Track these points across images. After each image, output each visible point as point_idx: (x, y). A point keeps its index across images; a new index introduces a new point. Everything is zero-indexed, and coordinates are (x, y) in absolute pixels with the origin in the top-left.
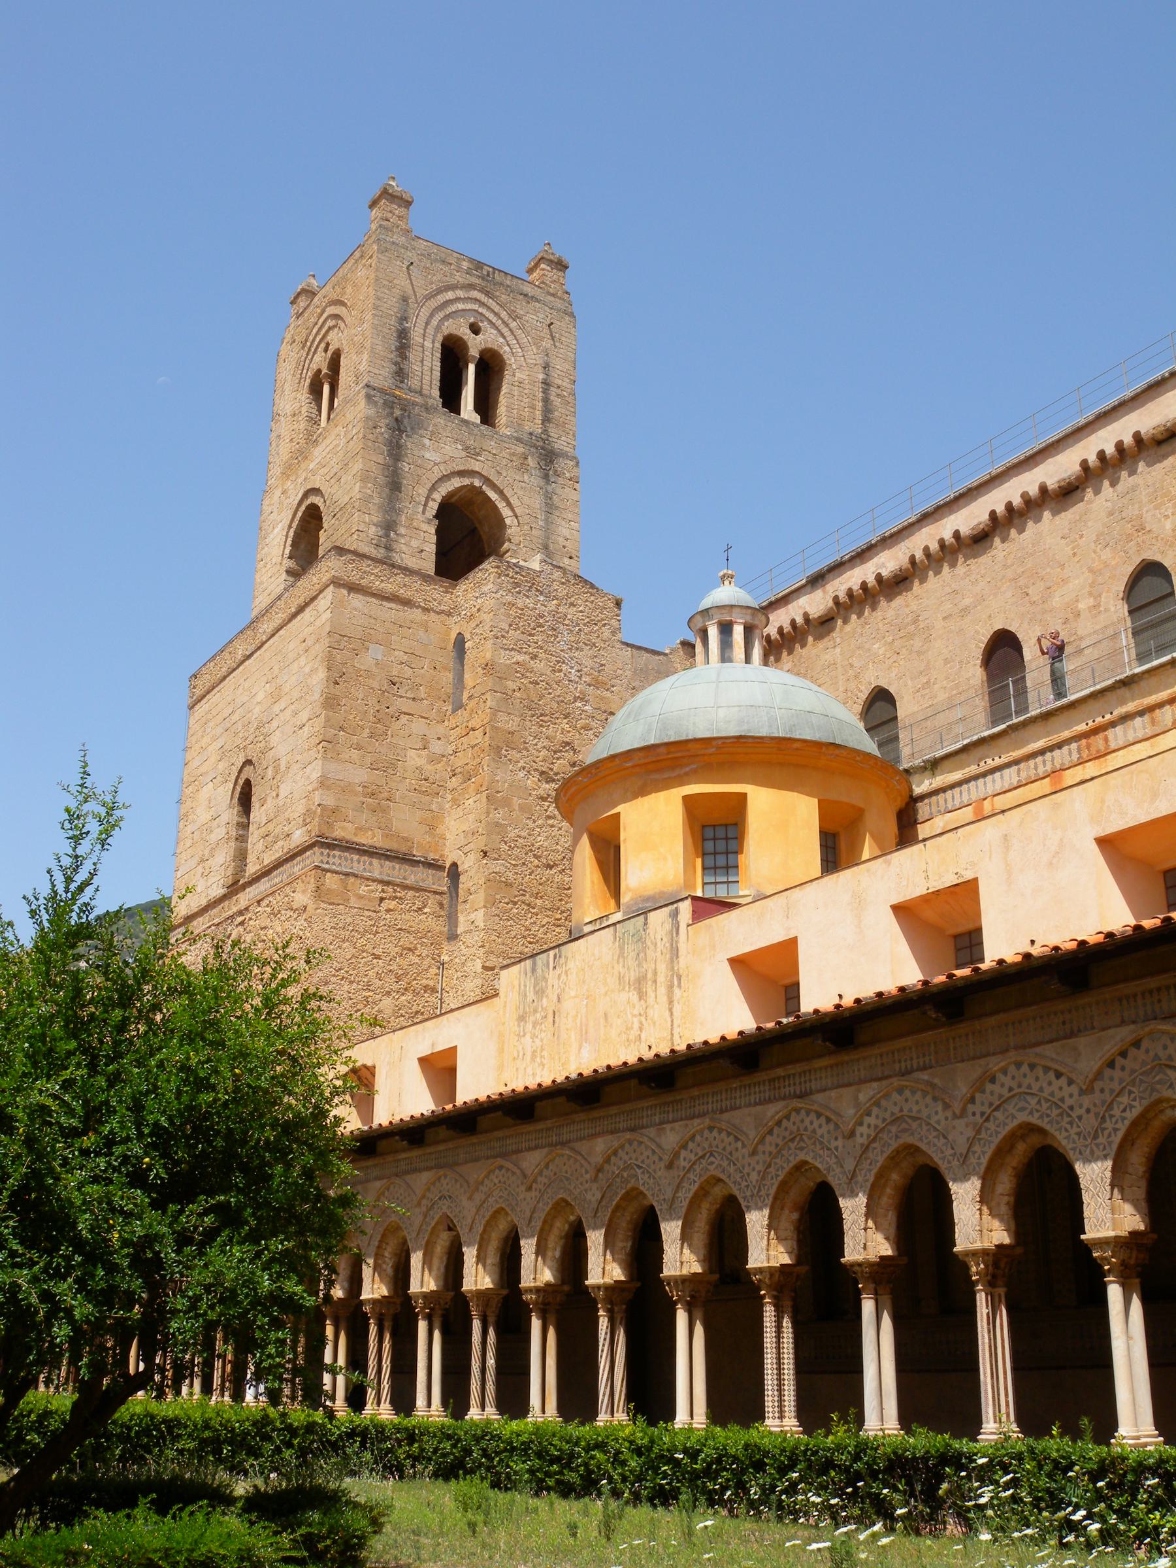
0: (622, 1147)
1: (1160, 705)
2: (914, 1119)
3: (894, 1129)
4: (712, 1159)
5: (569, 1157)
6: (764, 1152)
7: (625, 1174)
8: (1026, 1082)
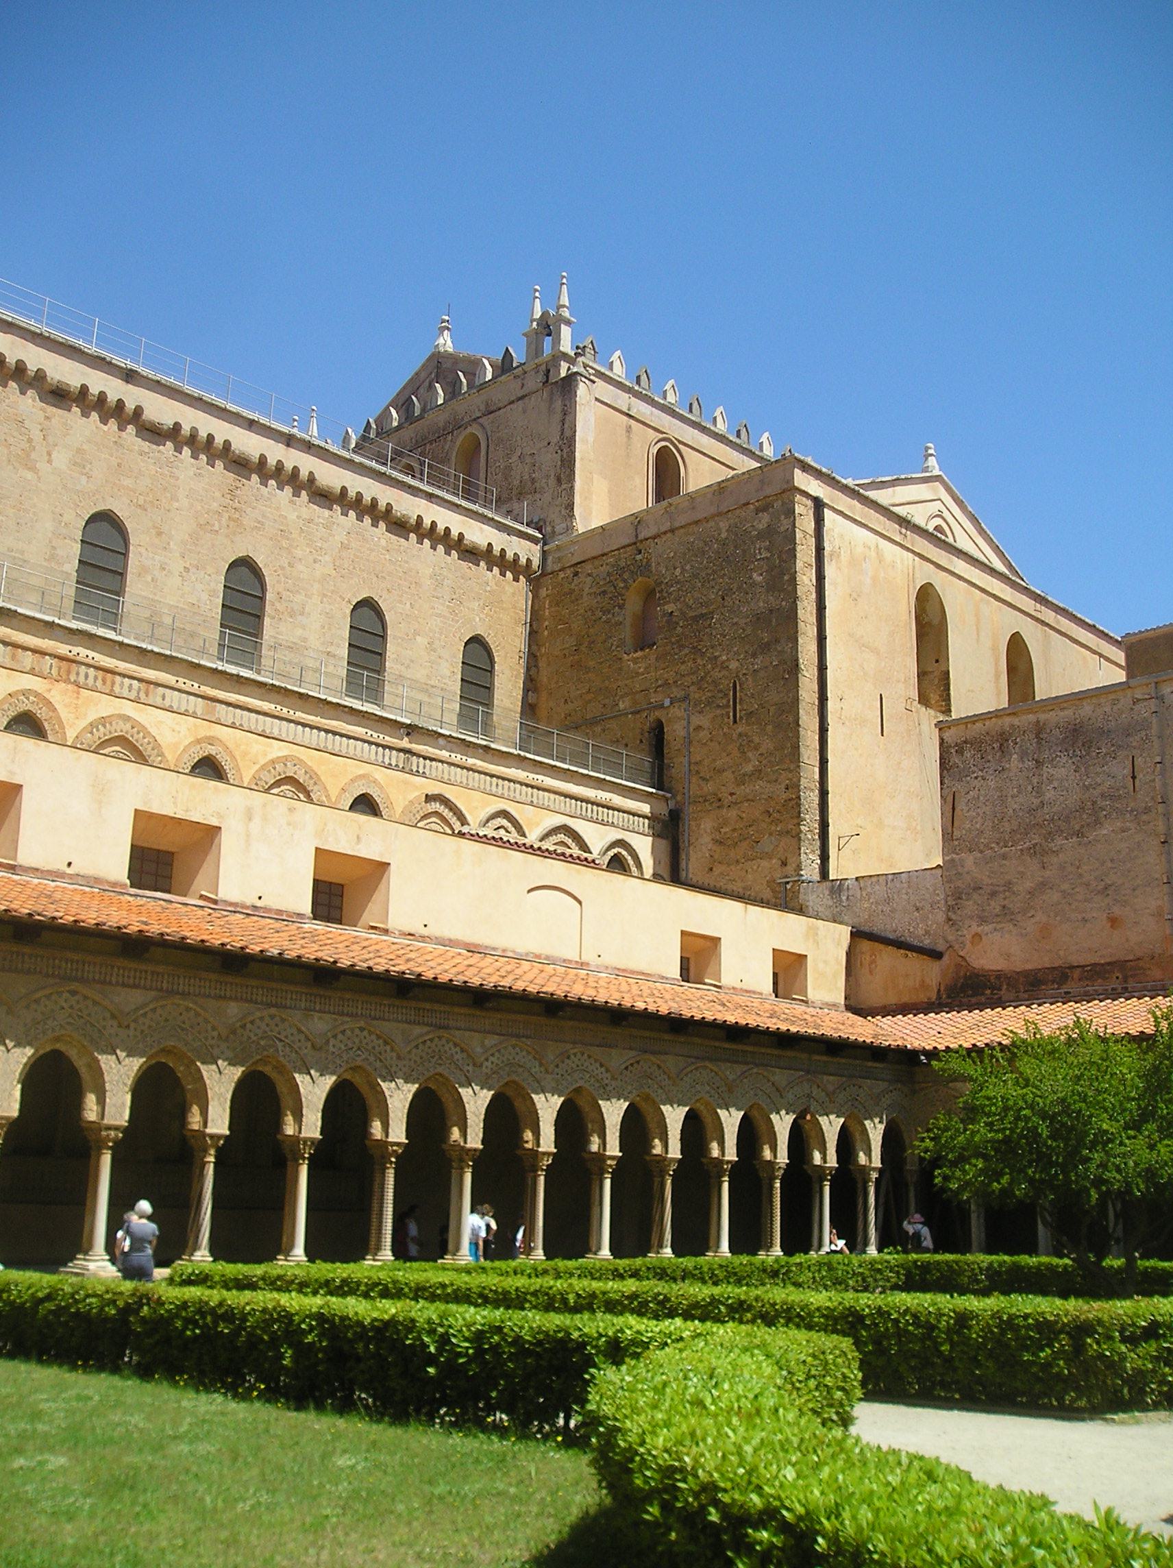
0: (262, 1019)
1: (25, 649)
2: (520, 1066)
3: (507, 1069)
4: (359, 1052)
5: (188, 1009)
6: (56, 1002)
7: (262, 1043)
8: (586, 1064)
